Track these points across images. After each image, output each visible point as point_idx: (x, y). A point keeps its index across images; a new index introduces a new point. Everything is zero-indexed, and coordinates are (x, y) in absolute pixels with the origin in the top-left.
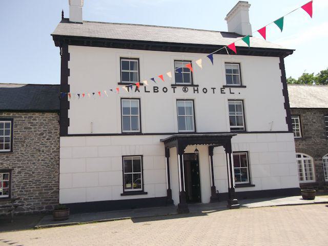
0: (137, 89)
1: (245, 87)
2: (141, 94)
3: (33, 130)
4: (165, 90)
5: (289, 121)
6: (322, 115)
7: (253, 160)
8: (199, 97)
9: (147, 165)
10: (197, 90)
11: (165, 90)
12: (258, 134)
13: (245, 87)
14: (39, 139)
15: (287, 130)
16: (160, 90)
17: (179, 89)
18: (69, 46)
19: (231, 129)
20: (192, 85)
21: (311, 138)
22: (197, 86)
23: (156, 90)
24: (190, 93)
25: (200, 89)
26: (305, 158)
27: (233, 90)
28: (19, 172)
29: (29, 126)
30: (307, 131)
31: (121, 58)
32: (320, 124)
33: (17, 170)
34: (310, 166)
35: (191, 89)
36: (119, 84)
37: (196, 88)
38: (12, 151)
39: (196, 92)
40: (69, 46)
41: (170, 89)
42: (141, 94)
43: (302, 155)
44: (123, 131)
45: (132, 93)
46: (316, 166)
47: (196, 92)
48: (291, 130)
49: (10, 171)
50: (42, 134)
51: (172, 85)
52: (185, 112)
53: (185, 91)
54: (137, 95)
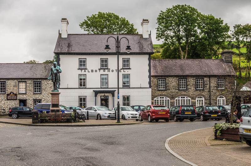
0: (85, 71)
1: (131, 69)
2: (87, 73)
3: (48, 86)
4: (96, 71)
5: (150, 83)
6: (178, 78)
7: (131, 99)
8: (110, 74)
9: (88, 99)
10: (109, 71)
11: (96, 71)
12: (135, 89)
13: (131, 69)
14: (50, 89)
15: (149, 87)
16: (94, 71)
17: (102, 71)
18: (60, 55)
19: (123, 86)
20: (107, 69)
21: (170, 89)
22: (109, 69)
23: (92, 71)
24: (106, 72)
25: (111, 70)
26: (166, 99)
27: (125, 70)
28: (44, 101)
29: (47, 84)
30: (168, 86)
31: (79, 59)
32: (176, 83)
33: (43, 100)
34: (168, 102)
35: (106, 70)
36: (78, 69)
37: (109, 70)
38: (41, 93)
39: (109, 72)
40: (60, 55)
41: (98, 71)
42: (87, 73)
43: (164, 97)
44: (80, 87)
45: (83, 72)
46: (171, 103)
47: (109, 72)
48: (150, 87)
49: (41, 100)
50: (51, 87)
51: (99, 69)
52: (104, 80)
53: (104, 71)
54: (85, 73)
